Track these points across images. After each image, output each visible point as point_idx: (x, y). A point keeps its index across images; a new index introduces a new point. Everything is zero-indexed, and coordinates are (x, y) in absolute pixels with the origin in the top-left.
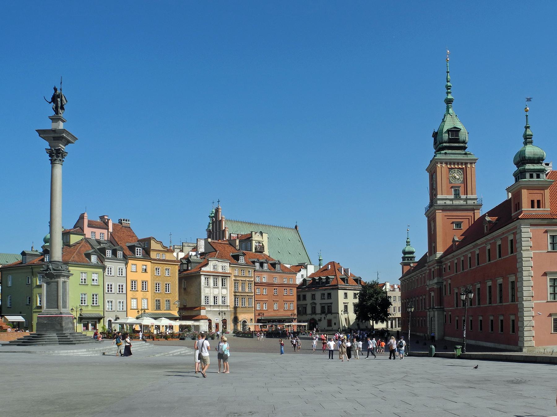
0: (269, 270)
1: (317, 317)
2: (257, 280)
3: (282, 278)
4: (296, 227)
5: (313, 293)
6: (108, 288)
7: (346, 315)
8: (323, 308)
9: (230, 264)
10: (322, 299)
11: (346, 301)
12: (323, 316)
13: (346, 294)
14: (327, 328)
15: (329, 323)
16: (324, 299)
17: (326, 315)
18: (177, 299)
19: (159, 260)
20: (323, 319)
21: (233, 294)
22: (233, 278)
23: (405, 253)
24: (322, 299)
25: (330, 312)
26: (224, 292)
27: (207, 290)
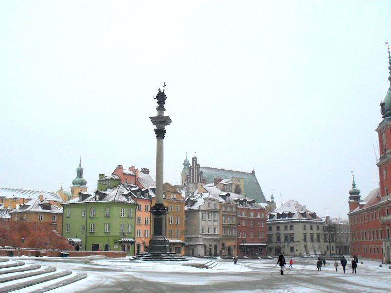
1: (281, 245)
4: (253, 172)
7: (305, 243)
8: (286, 237)
10: (285, 230)
11: (305, 232)
12: (287, 244)
13: (305, 226)
14: (290, 254)
15: (292, 249)
16: (287, 230)
17: (289, 243)
20: (286, 246)
22: (222, 213)
23: (351, 193)
24: (285, 230)
25: (292, 239)
26: (215, 223)
27: (203, 223)
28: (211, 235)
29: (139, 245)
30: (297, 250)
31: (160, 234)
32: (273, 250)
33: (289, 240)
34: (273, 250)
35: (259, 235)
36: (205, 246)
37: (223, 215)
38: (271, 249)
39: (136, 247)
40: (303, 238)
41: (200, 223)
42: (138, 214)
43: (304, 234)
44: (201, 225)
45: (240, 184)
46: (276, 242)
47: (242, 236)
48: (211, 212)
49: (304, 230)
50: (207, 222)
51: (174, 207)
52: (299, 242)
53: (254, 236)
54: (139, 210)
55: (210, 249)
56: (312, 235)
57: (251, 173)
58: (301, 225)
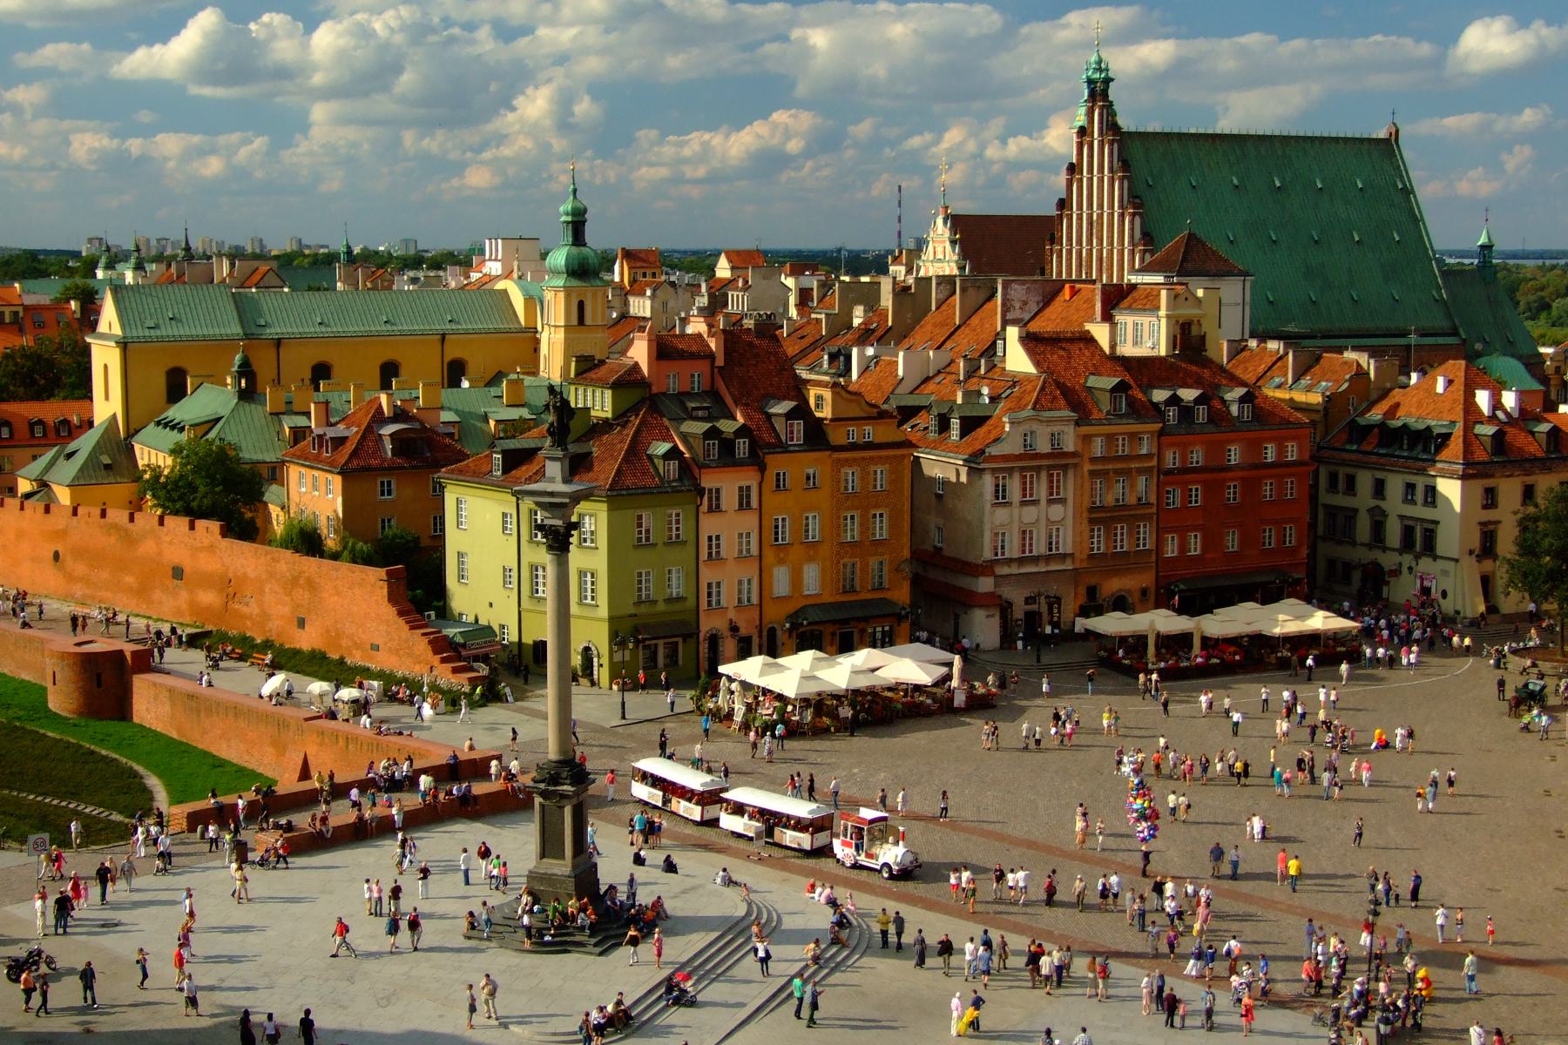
0: (1211, 428)
1: (1388, 560)
2: (1171, 459)
3: (1256, 446)
5: (1380, 475)
6: (710, 547)
7: (1488, 565)
8: (1408, 532)
9: (1077, 424)
10: (1405, 501)
12: (1407, 559)
16: (1413, 502)
17: (1417, 557)
18: (906, 553)
19: (854, 447)
20: (1405, 569)
21: (1085, 515)
22: (1087, 467)
24: (1405, 501)
25: (1429, 548)
26: (1057, 511)
27: (1002, 514)
28: (1036, 560)
29: (714, 640)
30: (1444, 594)
31: (562, 857)
32: (1356, 576)
33: (1418, 548)
34: (1356, 576)
35: (1270, 538)
36: (1005, 608)
37: (1093, 473)
38: (1348, 567)
39: (704, 648)
40: (1475, 543)
41: (987, 519)
42: (709, 525)
43: (1481, 524)
44: (987, 527)
45: (1204, 316)
46: (1370, 547)
47: (1183, 547)
48: (1038, 469)
49: (1485, 507)
50: (1016, 511)
51: (862, 479)
52: (1457, 561)
53: (1242, 543)
54: (715, 508)
55: (1032, 619)
56: (1525, 524)
57: (1382, 134)
58: (1478, 486)
